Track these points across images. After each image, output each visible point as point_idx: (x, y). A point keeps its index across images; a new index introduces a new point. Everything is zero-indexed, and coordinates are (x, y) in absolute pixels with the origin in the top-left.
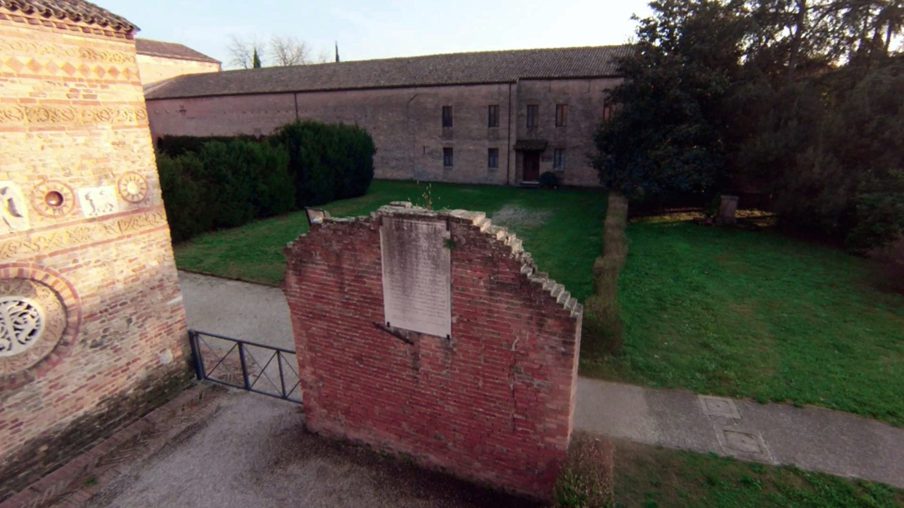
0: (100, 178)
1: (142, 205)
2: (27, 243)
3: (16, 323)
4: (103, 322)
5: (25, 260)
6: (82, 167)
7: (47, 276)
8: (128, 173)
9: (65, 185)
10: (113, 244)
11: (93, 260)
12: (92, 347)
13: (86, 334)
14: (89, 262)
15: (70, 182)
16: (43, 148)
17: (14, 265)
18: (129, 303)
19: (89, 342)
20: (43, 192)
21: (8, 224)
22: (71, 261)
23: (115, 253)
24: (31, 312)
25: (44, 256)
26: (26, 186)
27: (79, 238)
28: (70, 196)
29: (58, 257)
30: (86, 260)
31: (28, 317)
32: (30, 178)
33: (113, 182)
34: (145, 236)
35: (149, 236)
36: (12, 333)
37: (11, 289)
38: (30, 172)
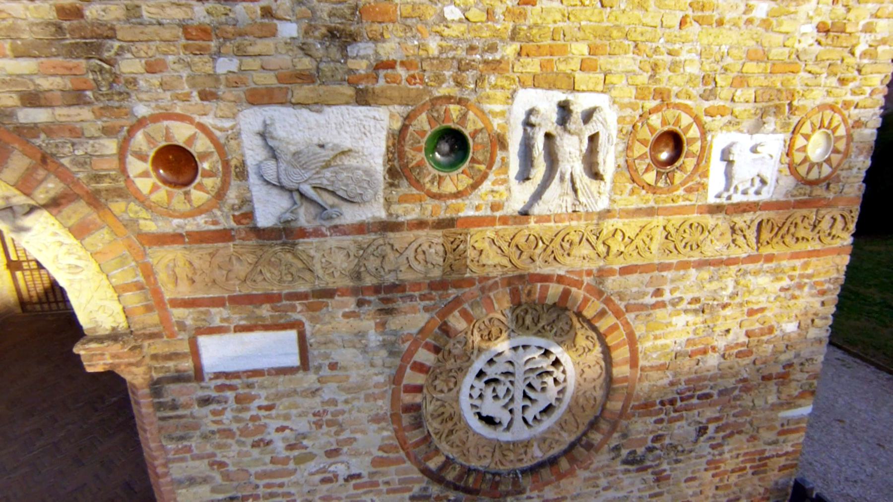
0: (764, 113)
1: (819, 191)
2: (593, 239)
3: (530, 386)
4: (661, 421)
5: (580, 273)
6: (741, 80)
7: (602, 314)
8: (822, 107)
9: (696, 119)
10: (733, 269)
11: (688, 297)
12: (625, 462)
13: (624, 436)
14: (681, 299)
15: (707, 113)
16: (682, 23)
17: (560, 279)
18: (716, 397)
19: (624, 452)
20: (652, 129)
21: (575, 190)
22: (651, 290)
23: (730, 290)
24: (558, 374)
25: (611, 272)
26: (628, 112)
27: (680, 246)
28: (696, 147)
29: (633, 278)
30: (677, 294)
31: (549, 380)
32: (641, 93)
33: (785, 126)
34: (798, 263)
35: (805, 266)
36: (519, 403)
37: (540, 325)
38: (643, 79)
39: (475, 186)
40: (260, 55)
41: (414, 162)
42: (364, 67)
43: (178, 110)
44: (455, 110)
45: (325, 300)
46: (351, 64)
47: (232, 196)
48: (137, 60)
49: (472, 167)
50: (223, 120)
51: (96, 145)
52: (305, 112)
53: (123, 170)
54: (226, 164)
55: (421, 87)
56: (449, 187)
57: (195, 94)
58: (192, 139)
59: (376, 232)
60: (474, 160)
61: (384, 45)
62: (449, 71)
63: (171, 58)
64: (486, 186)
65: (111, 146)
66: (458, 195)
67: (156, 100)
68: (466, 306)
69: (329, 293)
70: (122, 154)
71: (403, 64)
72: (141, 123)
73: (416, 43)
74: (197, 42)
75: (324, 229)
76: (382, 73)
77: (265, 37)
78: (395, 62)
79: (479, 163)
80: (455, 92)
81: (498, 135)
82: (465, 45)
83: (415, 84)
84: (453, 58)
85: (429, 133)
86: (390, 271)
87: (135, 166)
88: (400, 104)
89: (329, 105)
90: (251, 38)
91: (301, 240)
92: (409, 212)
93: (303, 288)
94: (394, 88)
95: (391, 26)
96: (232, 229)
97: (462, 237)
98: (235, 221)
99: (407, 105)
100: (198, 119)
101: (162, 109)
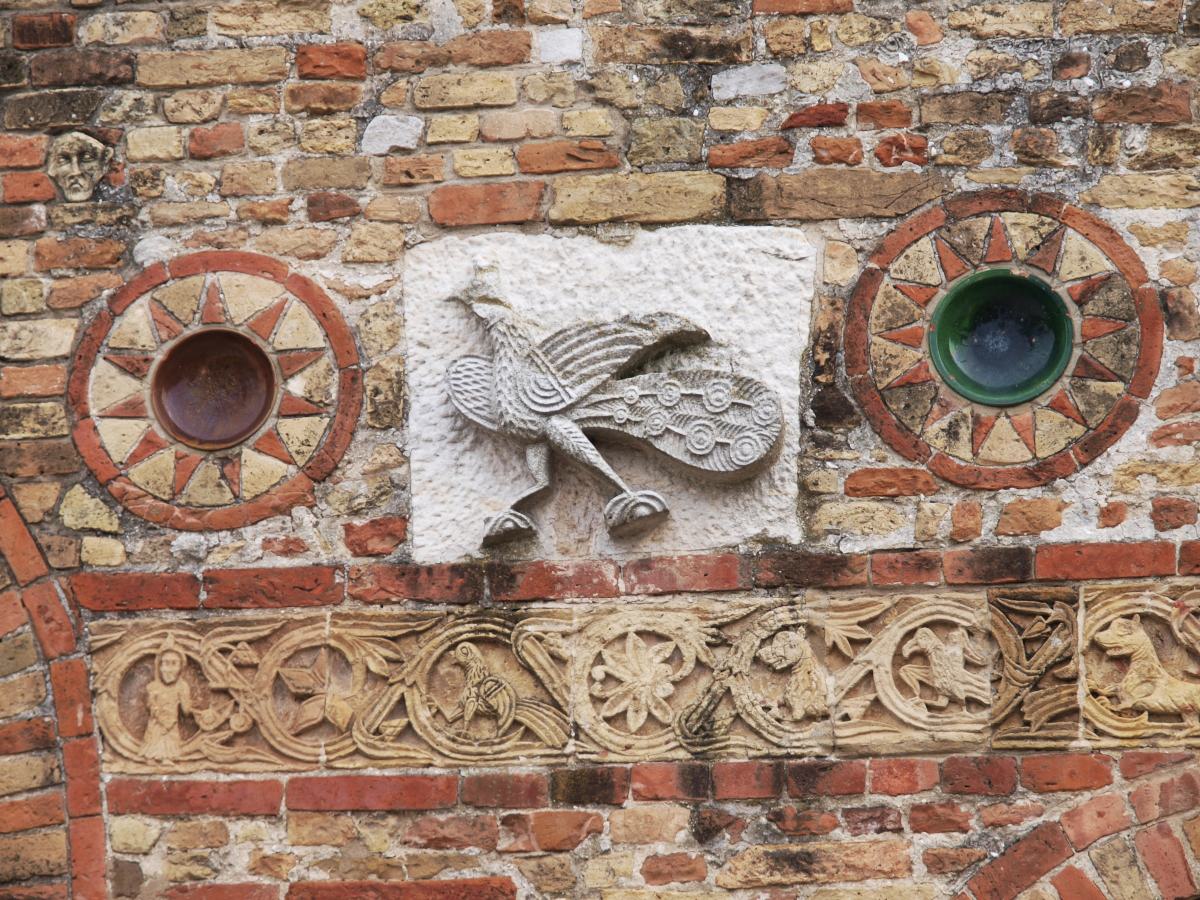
39: (1094, 446)
40: (477, 107)
41: (896, 373)
42: (756, 123)
43: (249, 248)
44: (1020, 230)
45: (590, 810)
46: (720, 119)
47: (354, 480)
48: (174, 128)
49: (1083, 389)
50: (362, 269)
51: (24, 334)
52: (585, 249)
53: (74, 400)
54: (351, 380)
55: (918, 170)
56: (1005, 446)
57: (300, 203)
58: (272, 316)
59: (771, 588)
60: (1089, 370)
61: (813, 67)
62: (1000, 123)
63: (254, 122)
64: (1133, 443)
65: (58, 337)
66: (1043, 473)
67: (200, 221)
68: (1082, 862)
69: (595, 786)
70: (80, 360)
71: (865, 112)
72: (152, 278)
73: (904, 57)
74: (327, 83)
75: (609, 572)
76: (804, 138)
77: (498, 64)
78: (842, 108)
79: (1103, 376)
80: (1026, 179)
81: (1164, 295)
82: (1046, 55)
83: (899, 162)
84: (1014, 91)
85: (942, 293)
86: (810, 718)
87: (107, 385)
88: (856, 217)
89: (651, 225)
90: (462, 68)
91: (537, 606)
92: (875, 531)
93: (526, 764)
94: (838, 176)
95: (833, 23)
96: (338, 567)
97: (1055, 613)
98: (350, 544)
99: (879, 218)
100: (295, 267)
101: (209, 242)
